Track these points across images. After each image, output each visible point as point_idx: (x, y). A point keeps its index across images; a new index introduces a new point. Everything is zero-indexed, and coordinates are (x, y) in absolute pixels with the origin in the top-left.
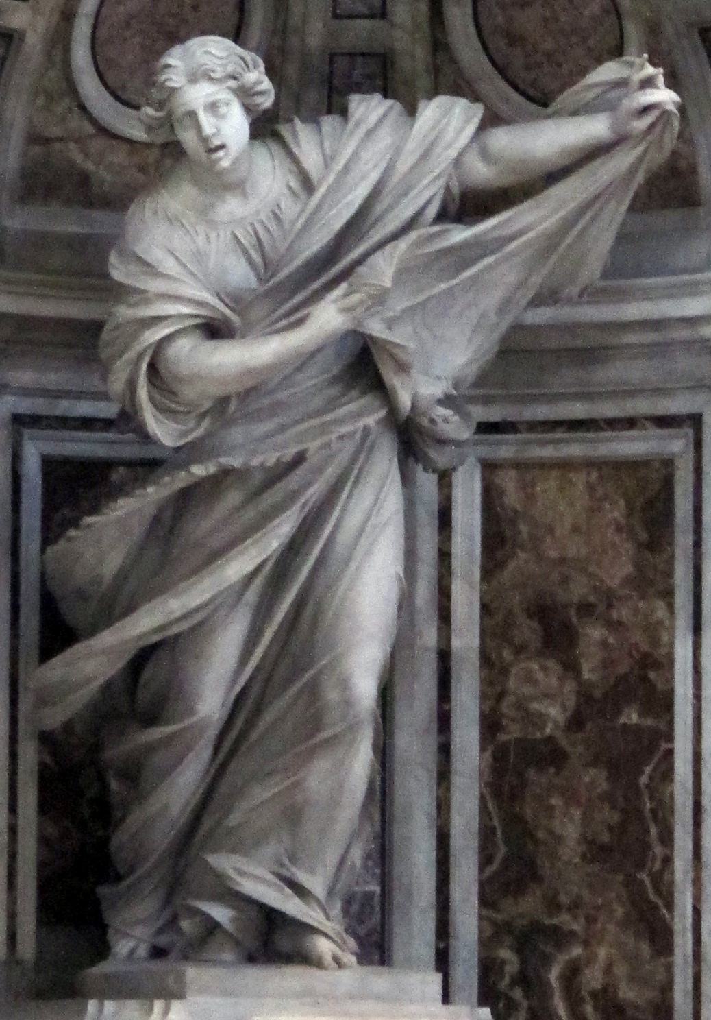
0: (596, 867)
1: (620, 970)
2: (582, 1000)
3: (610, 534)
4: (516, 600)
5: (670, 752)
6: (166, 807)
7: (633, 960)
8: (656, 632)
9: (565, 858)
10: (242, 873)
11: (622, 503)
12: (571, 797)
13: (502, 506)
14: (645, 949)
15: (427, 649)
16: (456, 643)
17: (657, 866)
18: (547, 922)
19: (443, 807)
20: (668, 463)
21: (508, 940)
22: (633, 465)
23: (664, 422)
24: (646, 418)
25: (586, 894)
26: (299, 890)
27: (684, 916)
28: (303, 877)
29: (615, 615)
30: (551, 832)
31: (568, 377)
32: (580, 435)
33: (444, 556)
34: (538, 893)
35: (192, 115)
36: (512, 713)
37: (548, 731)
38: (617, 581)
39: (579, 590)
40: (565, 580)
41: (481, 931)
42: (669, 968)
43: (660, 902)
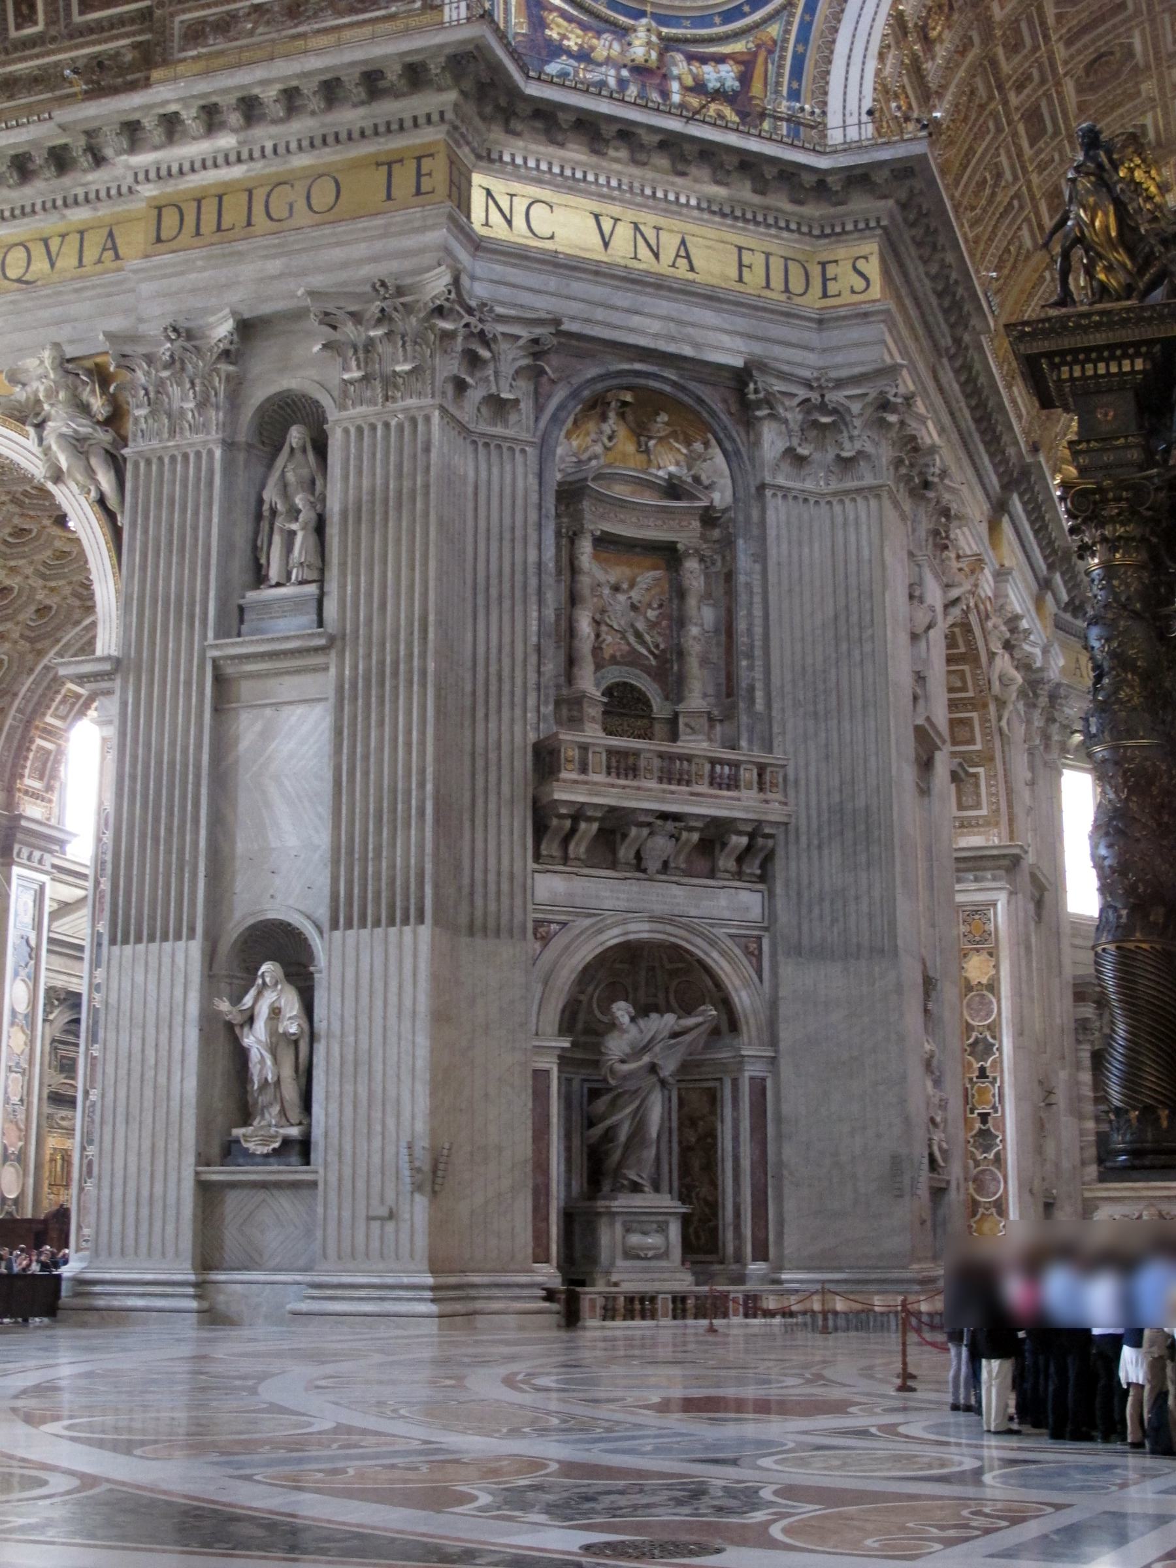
22: (709, 1089)
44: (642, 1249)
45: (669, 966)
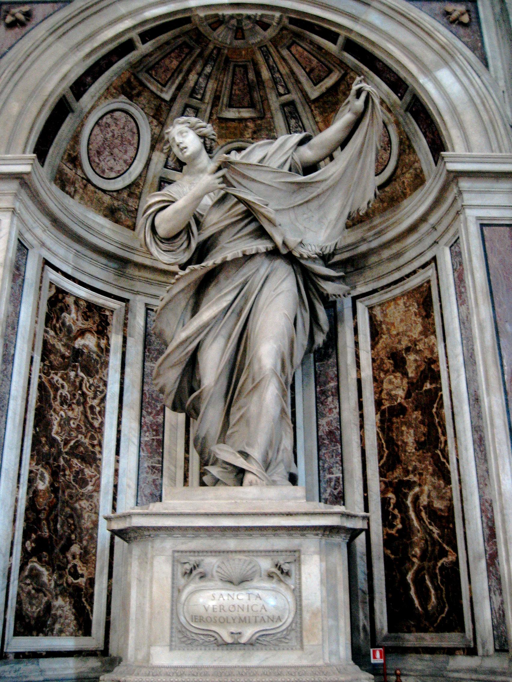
0: (421, 451)
1: (434, 494)
2: (421, 511)
3: (413, 318)
4: (383, 354)
5: (442, 395)
8: (432, 349)
10: (220, 450)
11: (415, 304)
12: (409, 426)
13: (377, 321)
14: (441, 482)
16: (363, 375)
17: (443, 445)
18: (405, 479)
19: (362, 439)
20: (429, 282)
21: (391, 489)
23: (423, 266)
24: (419, 268)
25: (417, 464)
26: (245, 455)
27: (453, 464)
28: (248, 450)
29: (418, 347)
30: (403, 441)
33: (357, 344)
36: (386, 397)
39: (405, 343)
40: (399, 342)
42: (451, 489)
43: (445, 461)
44: (224, 622)
45: (314, 93)
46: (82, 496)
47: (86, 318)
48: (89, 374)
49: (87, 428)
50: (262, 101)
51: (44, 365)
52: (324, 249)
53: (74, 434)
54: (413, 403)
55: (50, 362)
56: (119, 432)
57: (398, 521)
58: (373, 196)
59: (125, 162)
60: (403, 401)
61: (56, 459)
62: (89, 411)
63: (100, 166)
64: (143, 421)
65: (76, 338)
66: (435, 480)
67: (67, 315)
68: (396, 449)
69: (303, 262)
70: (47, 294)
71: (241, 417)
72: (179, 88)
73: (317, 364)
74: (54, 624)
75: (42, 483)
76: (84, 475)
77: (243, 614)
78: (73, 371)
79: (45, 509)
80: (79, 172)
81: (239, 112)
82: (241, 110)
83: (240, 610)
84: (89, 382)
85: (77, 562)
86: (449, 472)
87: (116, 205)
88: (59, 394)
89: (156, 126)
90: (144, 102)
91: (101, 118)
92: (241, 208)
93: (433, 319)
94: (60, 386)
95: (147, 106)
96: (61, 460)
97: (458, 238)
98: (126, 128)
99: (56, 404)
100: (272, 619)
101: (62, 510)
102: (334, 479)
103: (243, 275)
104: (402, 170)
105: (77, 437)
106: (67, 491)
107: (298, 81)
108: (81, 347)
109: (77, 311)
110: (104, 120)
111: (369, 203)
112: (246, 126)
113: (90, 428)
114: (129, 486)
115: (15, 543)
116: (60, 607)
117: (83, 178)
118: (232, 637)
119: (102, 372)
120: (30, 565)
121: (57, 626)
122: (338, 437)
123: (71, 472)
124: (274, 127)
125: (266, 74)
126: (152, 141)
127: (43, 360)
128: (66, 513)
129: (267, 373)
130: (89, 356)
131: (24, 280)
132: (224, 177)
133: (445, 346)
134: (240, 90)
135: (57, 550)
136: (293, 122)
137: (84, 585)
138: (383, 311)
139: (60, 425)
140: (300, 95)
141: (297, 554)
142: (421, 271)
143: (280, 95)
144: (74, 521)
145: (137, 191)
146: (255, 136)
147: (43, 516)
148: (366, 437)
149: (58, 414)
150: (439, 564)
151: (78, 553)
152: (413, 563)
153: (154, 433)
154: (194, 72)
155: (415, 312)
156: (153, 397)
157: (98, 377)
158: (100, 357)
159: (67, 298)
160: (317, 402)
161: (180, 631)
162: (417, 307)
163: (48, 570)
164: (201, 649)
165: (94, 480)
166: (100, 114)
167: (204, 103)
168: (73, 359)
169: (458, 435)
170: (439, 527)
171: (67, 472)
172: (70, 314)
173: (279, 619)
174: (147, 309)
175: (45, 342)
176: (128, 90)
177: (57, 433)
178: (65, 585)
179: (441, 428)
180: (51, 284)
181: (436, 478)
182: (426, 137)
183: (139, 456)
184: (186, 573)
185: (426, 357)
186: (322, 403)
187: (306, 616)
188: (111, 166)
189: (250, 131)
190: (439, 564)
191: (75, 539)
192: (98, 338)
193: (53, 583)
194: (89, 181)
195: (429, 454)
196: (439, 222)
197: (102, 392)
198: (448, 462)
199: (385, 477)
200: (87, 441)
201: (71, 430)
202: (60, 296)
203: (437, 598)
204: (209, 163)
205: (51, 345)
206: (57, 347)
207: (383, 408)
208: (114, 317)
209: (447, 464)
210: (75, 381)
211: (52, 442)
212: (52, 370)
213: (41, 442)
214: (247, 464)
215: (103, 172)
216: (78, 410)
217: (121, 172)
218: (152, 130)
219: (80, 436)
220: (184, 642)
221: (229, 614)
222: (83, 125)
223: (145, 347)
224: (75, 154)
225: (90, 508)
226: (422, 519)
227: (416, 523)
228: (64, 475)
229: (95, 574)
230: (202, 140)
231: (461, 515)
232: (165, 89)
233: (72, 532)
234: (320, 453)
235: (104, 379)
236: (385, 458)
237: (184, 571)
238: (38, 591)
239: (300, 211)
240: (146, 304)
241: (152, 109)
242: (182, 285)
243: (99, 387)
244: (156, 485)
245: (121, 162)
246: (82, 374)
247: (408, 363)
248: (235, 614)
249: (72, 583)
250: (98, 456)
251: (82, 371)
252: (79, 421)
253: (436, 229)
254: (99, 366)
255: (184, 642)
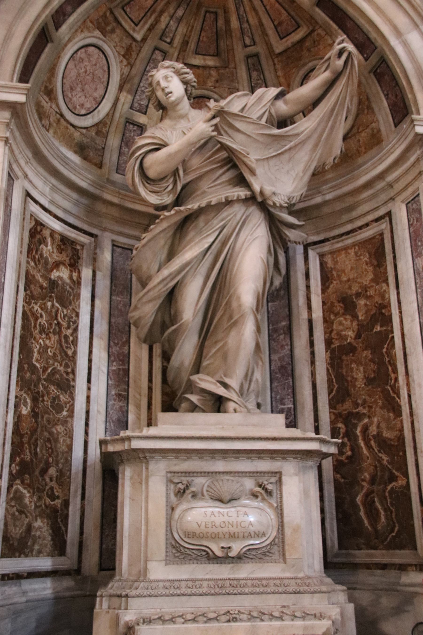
0: (370, 387)
2: (370, 440)
3: (364, 266)
4: (333, 298)
5: (393, 337)
6: (182, 363)
7: (388, 421)
8: (383, 295)
9: (359, 386)
10: (201, 380)
11: (367, 254)
12: (359, 363)
13: (327, 268)
14: (391, 414)
15: (304, 319)
16: (314, 316)
17: (393, 382)
18: (354, 411)
19: (313, 374)
20: (382, 234)
21: (340, 420)
22: (370, 240)
23: (377, 220)
24: (372, 221)
25: (367, 398)
26: (226, 386)
27: (404, 398)
28: (227, 380)
29: (368, 293)
30: (353, 377)
31: (345, 217)
32: (350, 235)
33: (308, 287)
34: (350, 400)
35: (158, 83)
36: (336, 337)
37: (349, 341)
38: (368, 282)
39: (355, 288)
40: (350, 288)
41: (330, 418)
43: (395, 396)
44: (215, 537)
46: (58, 421)
47: (60, 251)
48: (64, 305)
49: (62, 357)
50: (228, 51)
51: (26, 294)
52: (291, 199)
53: (51, 362)
54: (363, 343)
55: (31, 292)
56: (90, 361)
57: (348, 448)
58: (339, 152)
59: (95, 99)
60: (353, 341)
61: (36, 386)
62: (63, 340)
63: (73, 101)
64: (110, 351)
65: (52, 270)
66: (384, 412)
67: (44, 247)
68: (346, 384)
69: (272, 210)
70: (29, 225)
71: (218, 350)
72: (150, 29)
73: (270, 304)
74: (33, 545)
75: (24, 408)
76: (60, 401)
77: (233, 530)
78: (50, 301)
79: (27, 433)
80: (54, 106)
81: (205, 60)
82: (206, 57)
83: (230, 526)
84: (63, 312)
85: (54, 484)
86: (400, 406)
87: (85, 142)
88: (38, 323)
89: (125, 66)
90: (117, 40)
91: (76, 52)
92: (224, 154)
93: (386, 269)
94: (39, 315)
95: (118, 44)
96: (41, 386)
97: (419, 194)
98: (98, 65)
99: (36, 333)
100: (257, 535)
101: (42, 435)
102: (286, 409)
103: (222, 220)
104: (358, 129)
105: (53, 365)
106: (46, 416)
107: (264, 34)
108: (56, 279)
109: (52, 244)
110: (79, 53)
111: (335, 159)
112: (210, 75)
113: (65, 357)
114: (98, 412)
115: (4, 466)
116: (40, 528)
117: (56, 112)
118: (223, 551)
119: (75, 303)
120: (15, 487)
121: (36, 547)
122: (290, 372)
123: (49, 398)
124: (237, 78)
125: (235, 23)
126: (120, 80)
127: (25, 290)
128: (45, 437)
129: (246, 310)
130: (63, 288)
131: (11, 210)
132: (216, 125)
133: (398, 294)
134: (208, 37)
135: (37, 472)
136: (255, 74)
137: (59, 506)
138: (333, 260)
139: (39, 352)
140: (265, 47)
141: (278, 475)
142: (375, 224)
143: (246, 46)
144: (51, 444)
145: (104, 130)
146: (217, 85)
147: (25, 440)
148: (317, 372)
149: (37, 342)
150: (389, 488)
151: (55, 476)
152: (362, 487)
153: (121, 363)
154: (166, 14)
155: (366, 261)
156: (118, 329)
157: (71, 308)
158: (73, 290)
159: (44, 231)
160: (269, 340)
161: (174, 547)
162: (368, 256)
163: (29, 492)
164: (193, 563)
165: (68, 406)
166: (75, 48)
167: (172, 47)
168: (50, 290)
169: (410, 373)
170: (388, 455)
171: (46, 398)
172: (47, 246)
173: (264, 534)
174: (113, 245)
175: (27, 272)
176: (103, 25)
177: (37, 361)
178: (43, 506)
179: (391, 366)
180: (31, 215)
181: (386, 411)
182: (387, 99)
183: (108, 384)
184: (179, 492)
185: (377, 302)
186: (274, 340)
187: (288, 531)
188: (82, 102)
189: (213, 79)
190: (389, 488)
191: (52, 463)
192: (71, 271)
193: (33, 504)
194: (62, 115)
195: (379, 389)
196: (397, 180)
197: (75, 322)
198: (399, 398)
199: (336, 409)
200: (62, 369)
201: (48, 358)
202: (39, 228)
203: (386, 518)
204: (189, 110)
205: (31, 275)
206: (36, 277)
207: (333, 346)
208: (85, 251)
209: (397, 399)
210: (51, 311)
211: (33, 369)
212: (33, 299)
213: (24, 368)
214: (228, 393)
215: (75, 108)
216: (54, 338)
217: (91, 110)
218: (121, 69)
219: (56, 364)
220: (178, 557)
221: (220, 530)
222: (59, 57)
223: (112, 282)
224: (50, 87)
225: (65, 432)
226: (371, 447)
227: (365, 451)
228: (43, 401)
229: (69, 496)
230: (185, 87)
231: (412, 444)
232: (137, 28)
233: (50, 456)
234: (273, 385)
235: (76, 310)
236: (334, 392)
237: (177, 490)
238: (21, 512)
239: (272, 162)
240: (113, 241)
241: (123, 47)
242: (165, 225)
243: (72, 317)
244: (123, 412)
245: (91, 99)
246: (57, 305)
247: (358, 307)
248: (225, 530)
249: (50, 504)
250: (72, 383)
251: (57, 301)
252: (55, 350)
253: (392, 187)
254: (72, 297)
255: (178, 557)
